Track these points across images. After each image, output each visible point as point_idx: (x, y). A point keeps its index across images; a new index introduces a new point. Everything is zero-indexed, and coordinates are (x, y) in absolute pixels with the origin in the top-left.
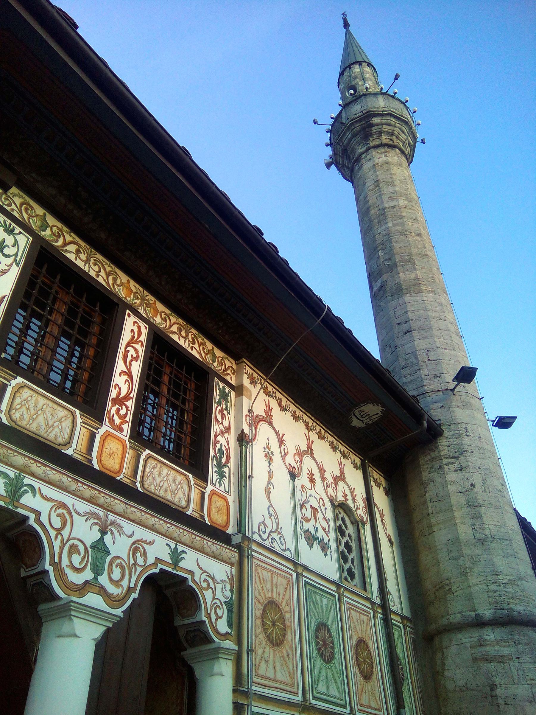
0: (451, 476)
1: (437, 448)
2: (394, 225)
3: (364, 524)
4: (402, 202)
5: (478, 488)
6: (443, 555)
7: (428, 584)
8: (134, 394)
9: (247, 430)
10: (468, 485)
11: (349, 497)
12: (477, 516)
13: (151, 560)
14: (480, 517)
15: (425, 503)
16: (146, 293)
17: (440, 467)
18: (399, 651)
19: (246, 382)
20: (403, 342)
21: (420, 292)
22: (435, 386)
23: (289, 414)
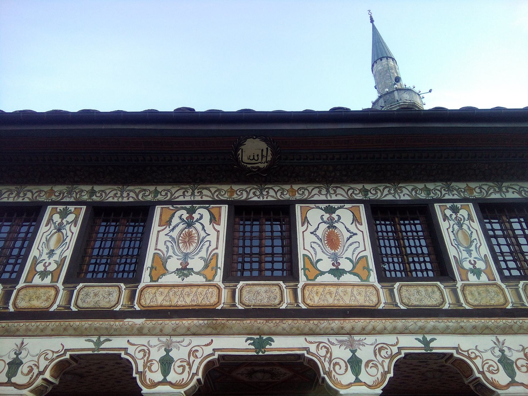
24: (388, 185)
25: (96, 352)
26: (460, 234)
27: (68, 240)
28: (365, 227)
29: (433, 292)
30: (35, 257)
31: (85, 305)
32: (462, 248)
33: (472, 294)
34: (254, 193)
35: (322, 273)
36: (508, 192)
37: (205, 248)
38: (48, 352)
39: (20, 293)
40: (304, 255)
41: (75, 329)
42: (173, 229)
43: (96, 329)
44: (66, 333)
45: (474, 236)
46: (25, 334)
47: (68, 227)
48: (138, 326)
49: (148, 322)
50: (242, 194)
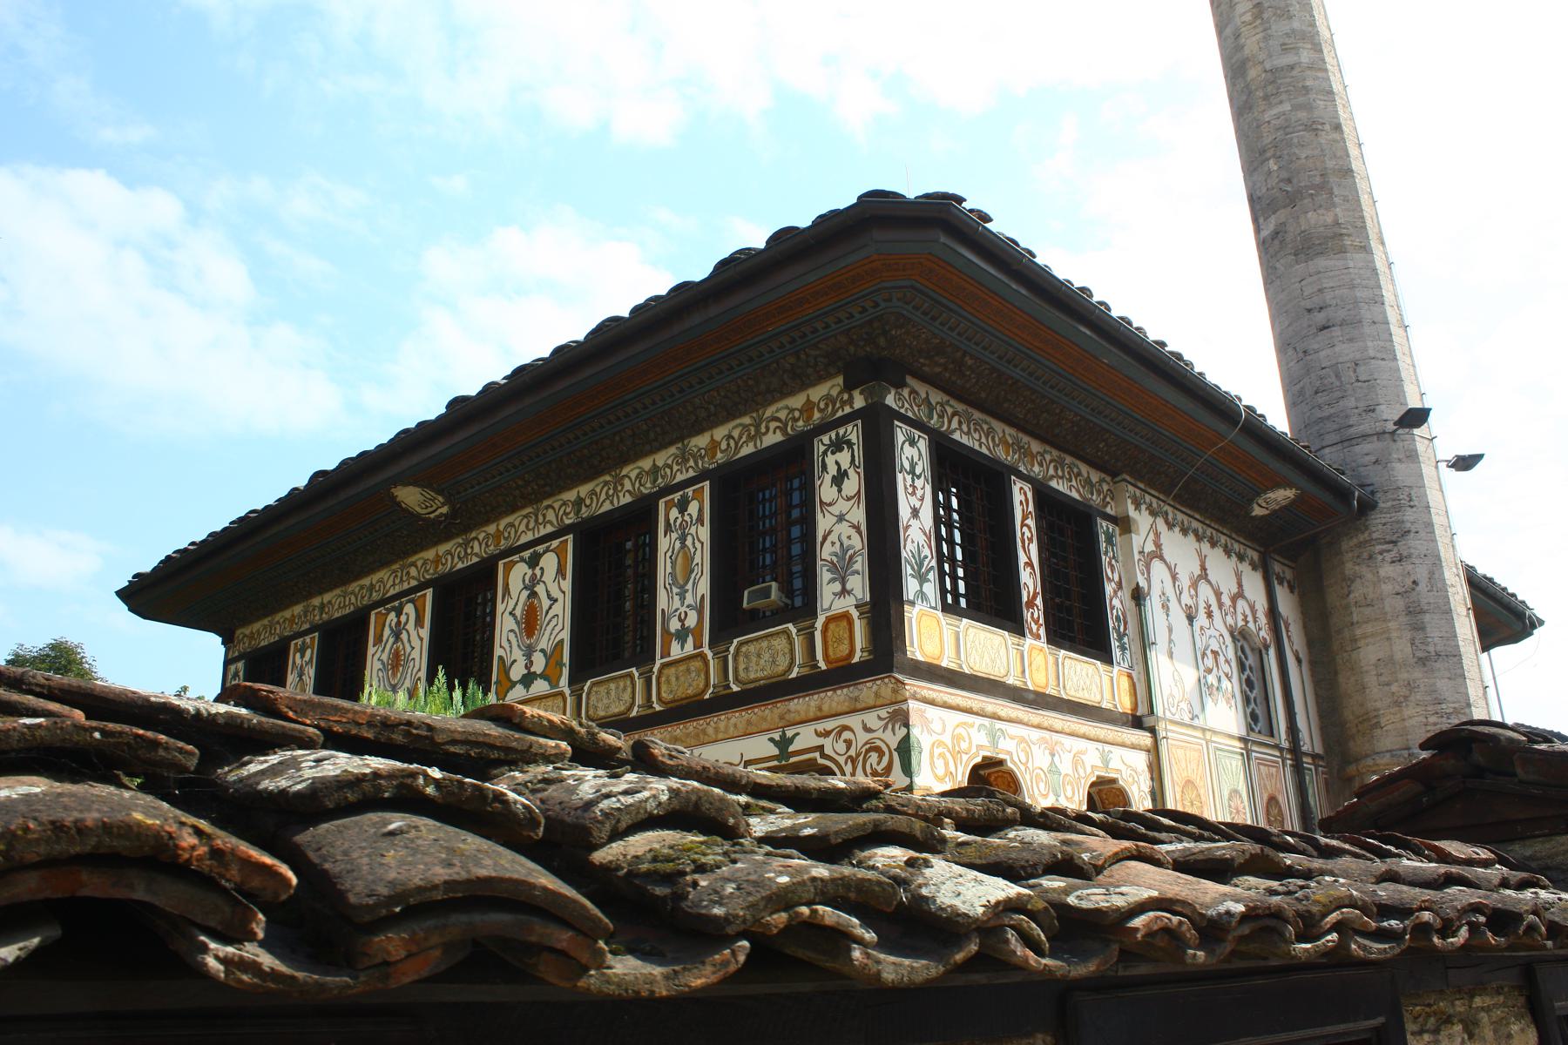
0: (1387, 570)
1: (1367, 528)
2: (1296, 108)
3: (1267, 647)
4: (1305, 56)
5: (1422, 587)
6: (1371, 680)
7: (1348, 714)
8: (1039, 589)
9: (1143, 583)
10: (1408, 582)
11: (1250, 618)
12: (1419, 628)
13: (1089, 770)
14: (1423, 629)
15: (1347, 607)
16: (1020, 435)
17: (1370, 557)
18: (1311, 800)
19: (1132, 512)
20: (1316, 346)
21: (1343, 250)
22: (1365, 427)
23: (1177, 529)
24: (608, 478)
26: (680, 560)
28: (567, 585)
29: (625, 689)
32: (675, 590)
33: (668, 681)
35: (513, 684)
36: (768, 429)
40: (501, 658)
45: (697, 559)
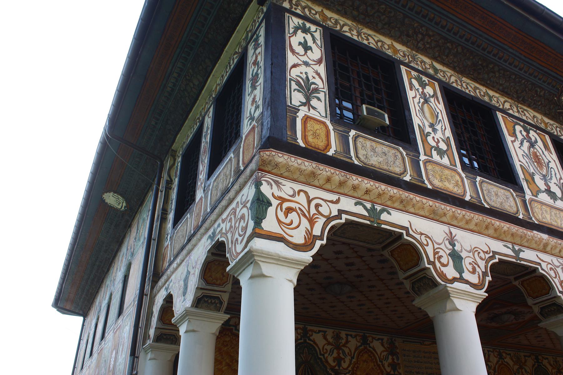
25: (518, 262)
27: (440, 117)
30: (419, 125)
31: (493, 204)
34: (560, 131)
37: (553, 175)
38: (479, 251)
39: (428, 168)
41: (496, 230)
42: (522, 143)
43: (512, 235)
44: (486, 232)
46: (450, 221)
47: (432, 100)
48: (544, 241)
49: (551, 240)
50: (552, 129)
